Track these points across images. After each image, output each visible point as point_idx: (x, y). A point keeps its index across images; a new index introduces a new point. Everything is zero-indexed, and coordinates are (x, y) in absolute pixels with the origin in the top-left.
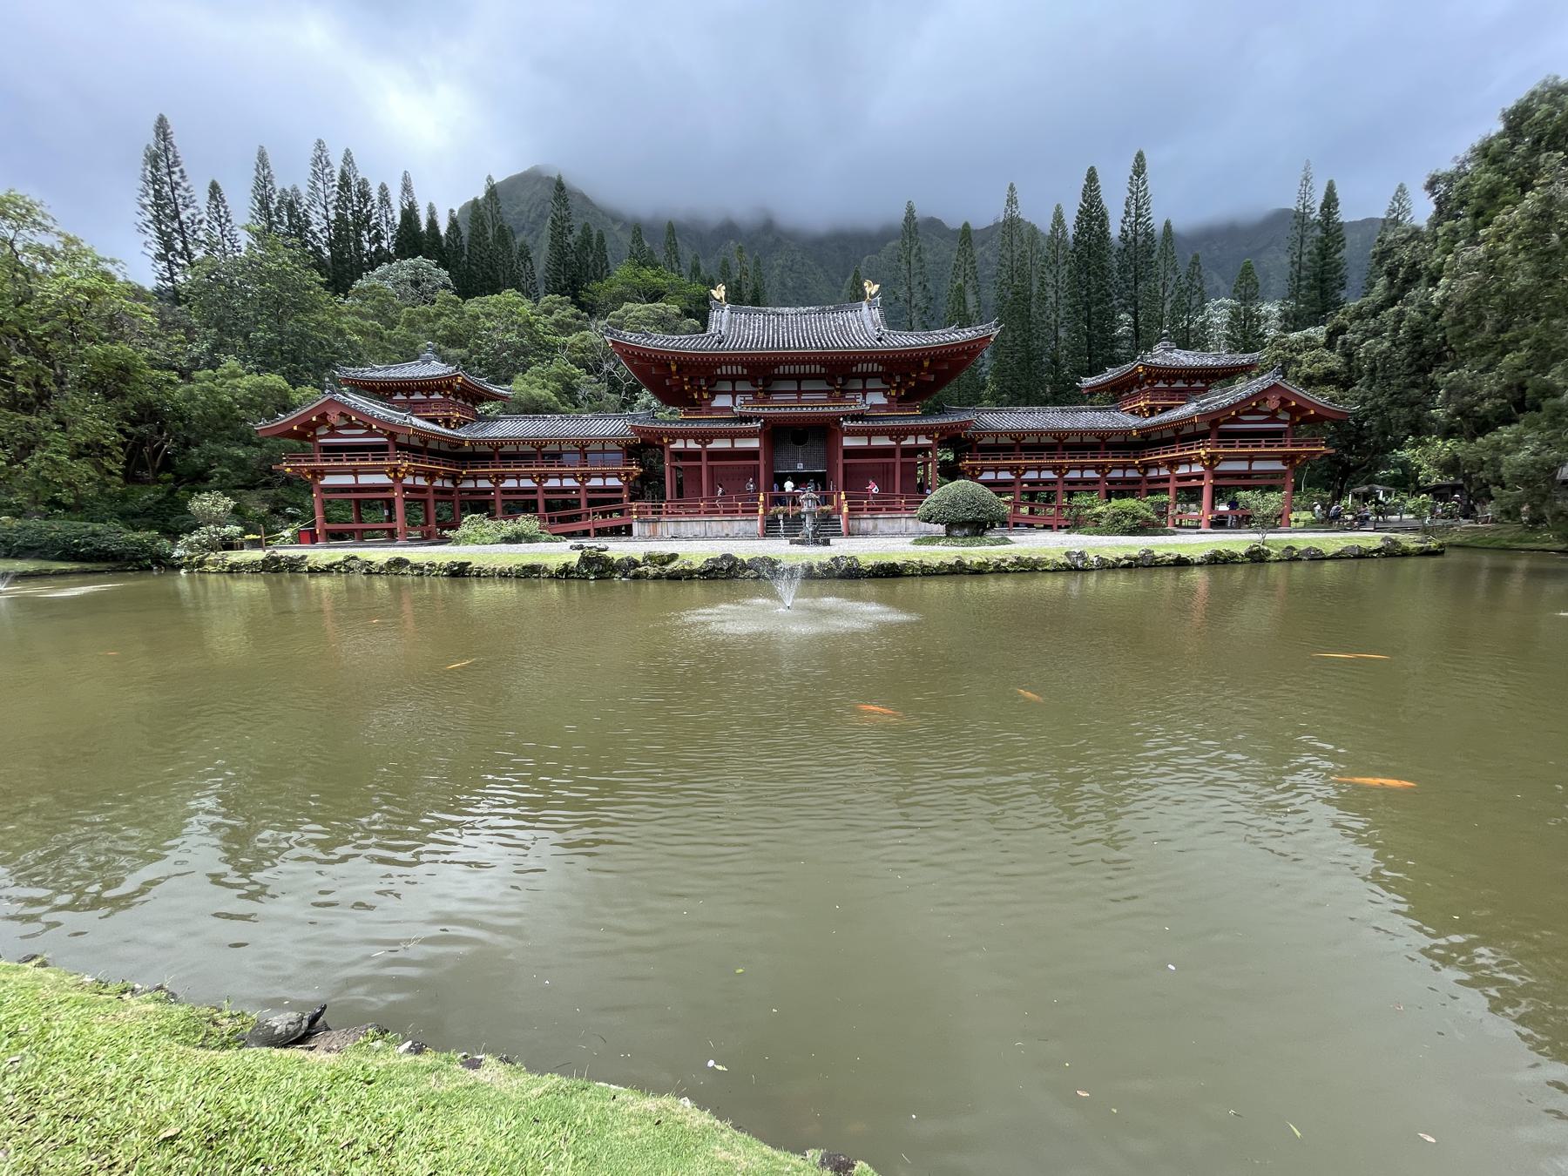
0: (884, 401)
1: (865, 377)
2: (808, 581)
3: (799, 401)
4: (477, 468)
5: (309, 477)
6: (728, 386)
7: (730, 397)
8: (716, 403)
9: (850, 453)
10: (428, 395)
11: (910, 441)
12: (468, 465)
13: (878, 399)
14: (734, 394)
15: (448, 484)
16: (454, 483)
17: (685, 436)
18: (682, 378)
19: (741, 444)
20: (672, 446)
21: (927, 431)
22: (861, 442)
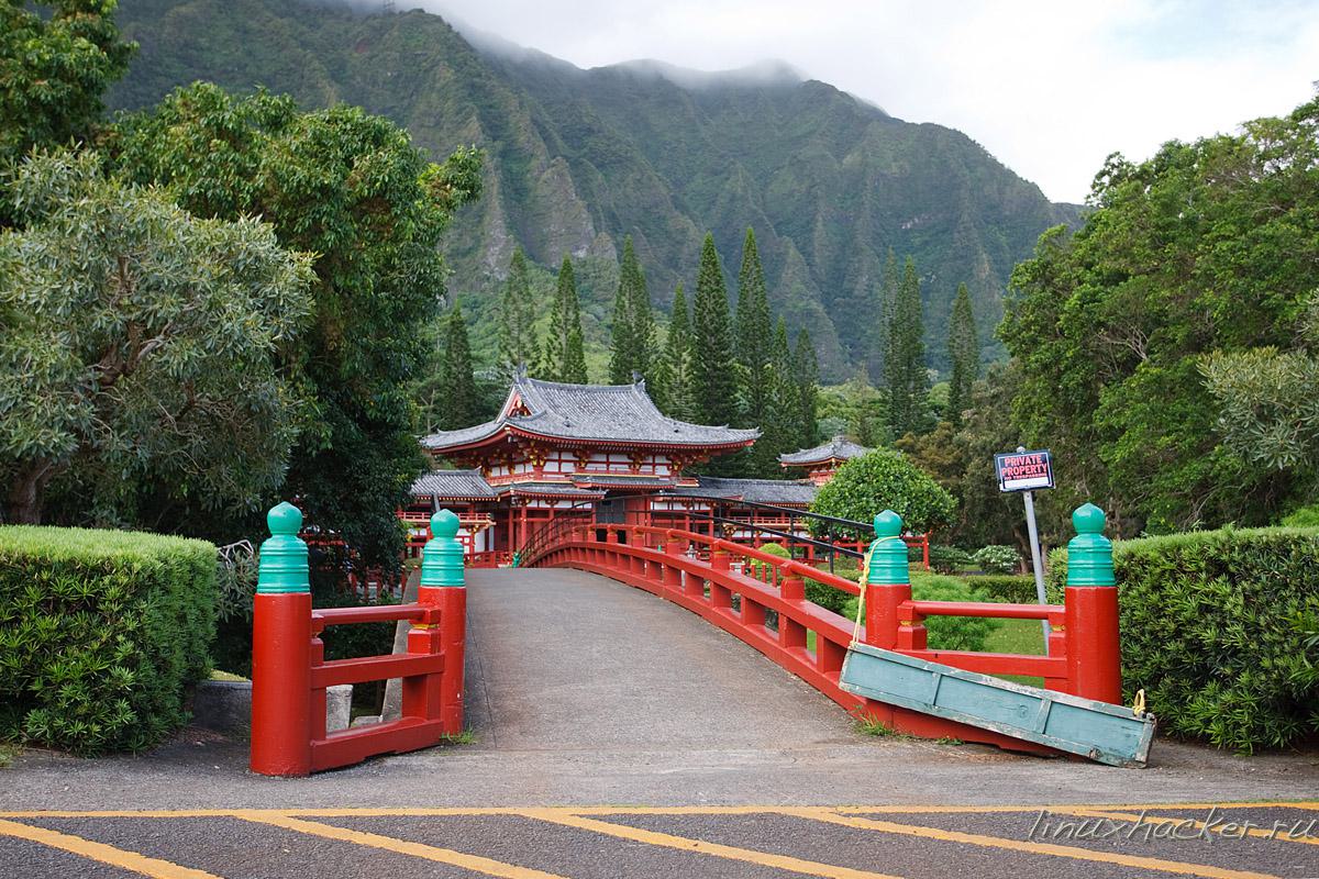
0: (668, 473)
3: (608, 471)
7: (557, 464)
9: (657, 515)
14: (560, 461)
17: (538, 498)
21: (709, 501)
22: (664, 507)
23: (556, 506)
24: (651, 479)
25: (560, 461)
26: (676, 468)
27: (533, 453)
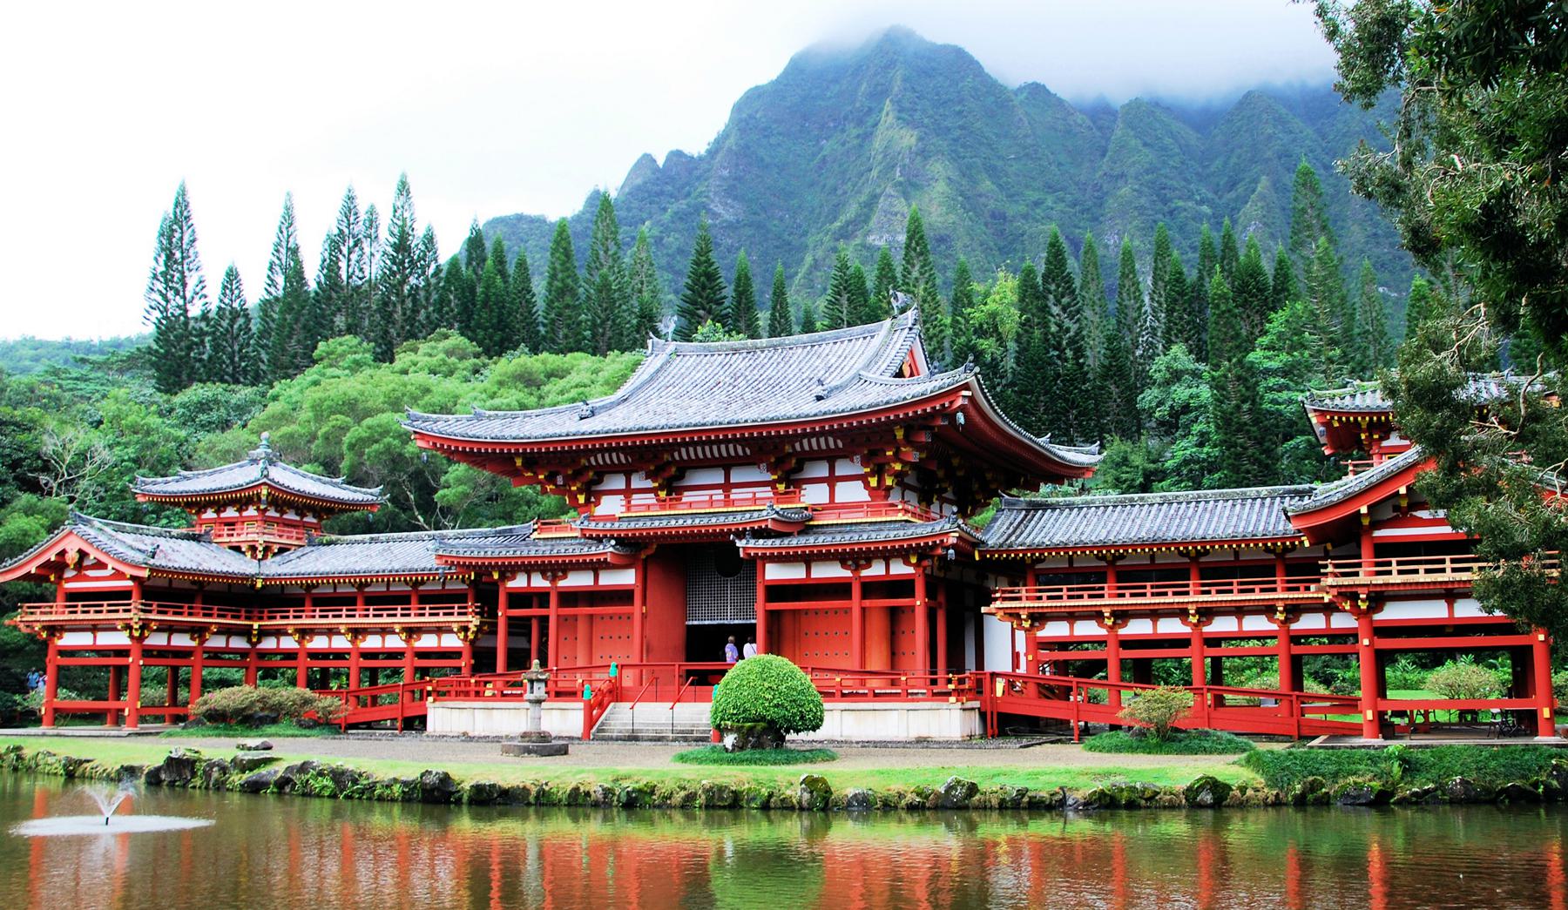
1: (831, 457)
2: (429, 807)
4: (275, 618)
5: (44, 635)
6: (618, 483)
10: (240, 510)
11: (876, 570)
12: (266, 614)
13: (853, 492)
14: (628, 492)
15: (238, 643)
16: (249, 641)
17: (529, 568)
18: (536, 474)
19: (609, 579)
20: (510, 584)
22: (795, 573)
23: (561, 583)
25: (628, 492)
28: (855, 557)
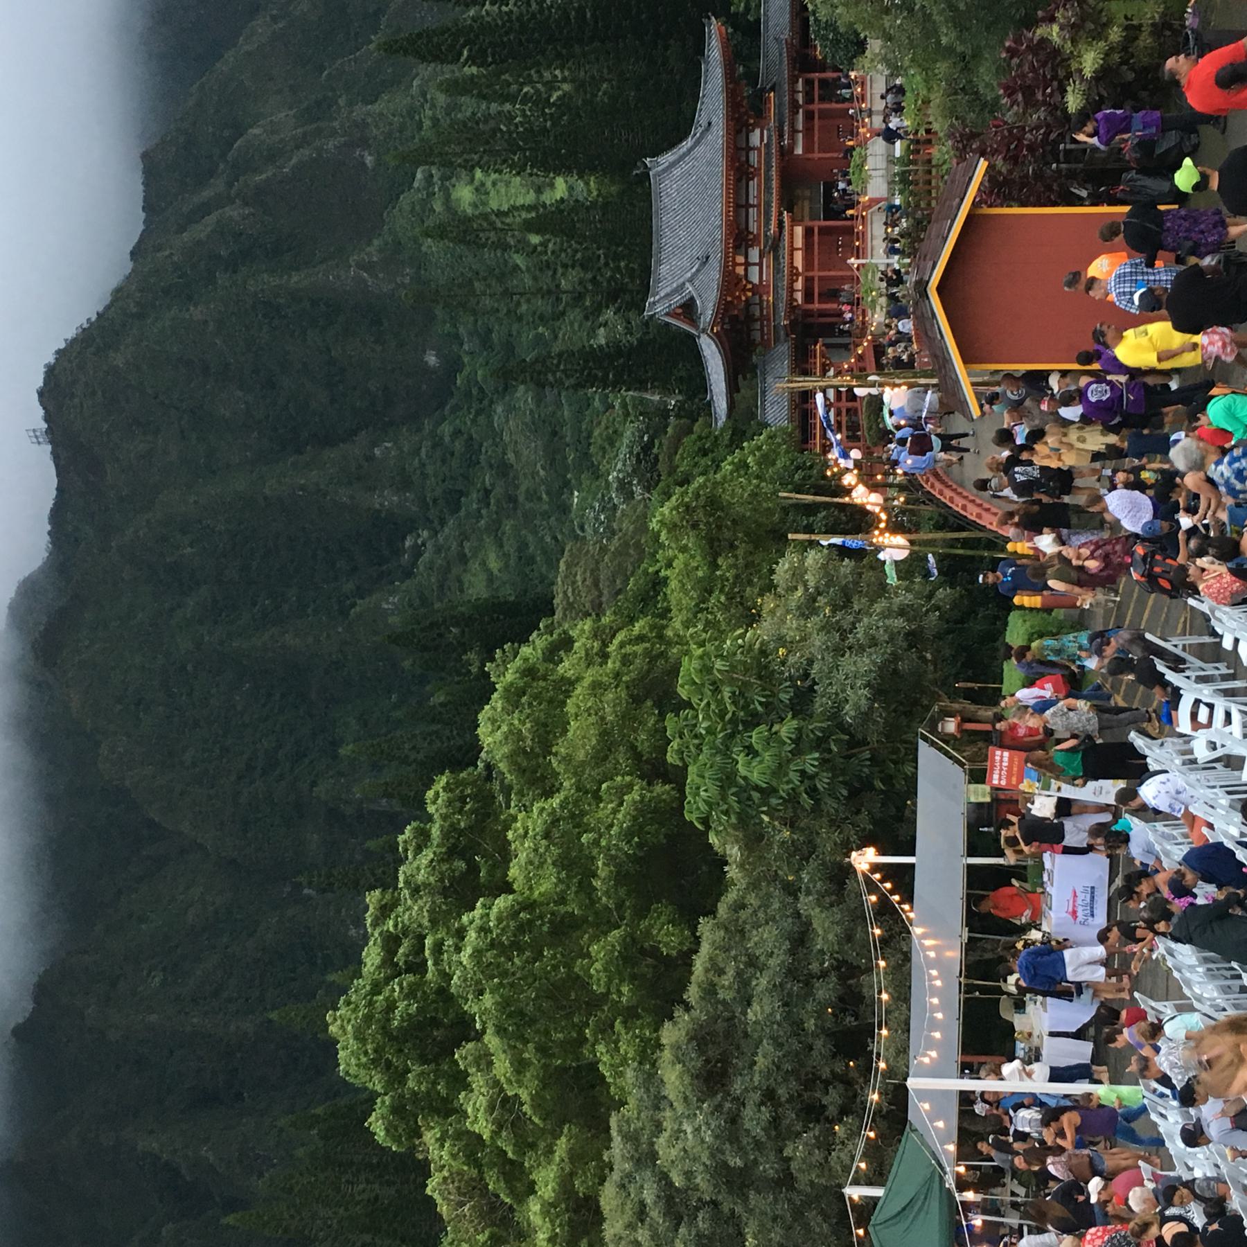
0: (758, 131)
3: (758, 206)
7: (750, 269)
8: (756, 280)
9: (808, 148)
14: (747, 264)
19: (799, 242)
21: (793, 81)
24: (768, 154)
26: (752, 121)
27: (739, 297)
28: (795, 106)
